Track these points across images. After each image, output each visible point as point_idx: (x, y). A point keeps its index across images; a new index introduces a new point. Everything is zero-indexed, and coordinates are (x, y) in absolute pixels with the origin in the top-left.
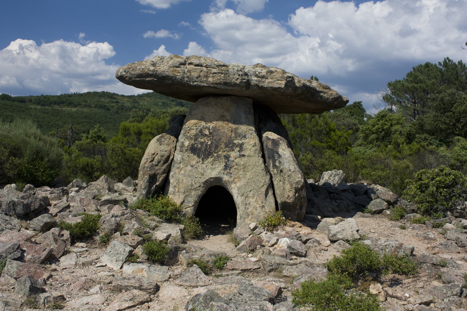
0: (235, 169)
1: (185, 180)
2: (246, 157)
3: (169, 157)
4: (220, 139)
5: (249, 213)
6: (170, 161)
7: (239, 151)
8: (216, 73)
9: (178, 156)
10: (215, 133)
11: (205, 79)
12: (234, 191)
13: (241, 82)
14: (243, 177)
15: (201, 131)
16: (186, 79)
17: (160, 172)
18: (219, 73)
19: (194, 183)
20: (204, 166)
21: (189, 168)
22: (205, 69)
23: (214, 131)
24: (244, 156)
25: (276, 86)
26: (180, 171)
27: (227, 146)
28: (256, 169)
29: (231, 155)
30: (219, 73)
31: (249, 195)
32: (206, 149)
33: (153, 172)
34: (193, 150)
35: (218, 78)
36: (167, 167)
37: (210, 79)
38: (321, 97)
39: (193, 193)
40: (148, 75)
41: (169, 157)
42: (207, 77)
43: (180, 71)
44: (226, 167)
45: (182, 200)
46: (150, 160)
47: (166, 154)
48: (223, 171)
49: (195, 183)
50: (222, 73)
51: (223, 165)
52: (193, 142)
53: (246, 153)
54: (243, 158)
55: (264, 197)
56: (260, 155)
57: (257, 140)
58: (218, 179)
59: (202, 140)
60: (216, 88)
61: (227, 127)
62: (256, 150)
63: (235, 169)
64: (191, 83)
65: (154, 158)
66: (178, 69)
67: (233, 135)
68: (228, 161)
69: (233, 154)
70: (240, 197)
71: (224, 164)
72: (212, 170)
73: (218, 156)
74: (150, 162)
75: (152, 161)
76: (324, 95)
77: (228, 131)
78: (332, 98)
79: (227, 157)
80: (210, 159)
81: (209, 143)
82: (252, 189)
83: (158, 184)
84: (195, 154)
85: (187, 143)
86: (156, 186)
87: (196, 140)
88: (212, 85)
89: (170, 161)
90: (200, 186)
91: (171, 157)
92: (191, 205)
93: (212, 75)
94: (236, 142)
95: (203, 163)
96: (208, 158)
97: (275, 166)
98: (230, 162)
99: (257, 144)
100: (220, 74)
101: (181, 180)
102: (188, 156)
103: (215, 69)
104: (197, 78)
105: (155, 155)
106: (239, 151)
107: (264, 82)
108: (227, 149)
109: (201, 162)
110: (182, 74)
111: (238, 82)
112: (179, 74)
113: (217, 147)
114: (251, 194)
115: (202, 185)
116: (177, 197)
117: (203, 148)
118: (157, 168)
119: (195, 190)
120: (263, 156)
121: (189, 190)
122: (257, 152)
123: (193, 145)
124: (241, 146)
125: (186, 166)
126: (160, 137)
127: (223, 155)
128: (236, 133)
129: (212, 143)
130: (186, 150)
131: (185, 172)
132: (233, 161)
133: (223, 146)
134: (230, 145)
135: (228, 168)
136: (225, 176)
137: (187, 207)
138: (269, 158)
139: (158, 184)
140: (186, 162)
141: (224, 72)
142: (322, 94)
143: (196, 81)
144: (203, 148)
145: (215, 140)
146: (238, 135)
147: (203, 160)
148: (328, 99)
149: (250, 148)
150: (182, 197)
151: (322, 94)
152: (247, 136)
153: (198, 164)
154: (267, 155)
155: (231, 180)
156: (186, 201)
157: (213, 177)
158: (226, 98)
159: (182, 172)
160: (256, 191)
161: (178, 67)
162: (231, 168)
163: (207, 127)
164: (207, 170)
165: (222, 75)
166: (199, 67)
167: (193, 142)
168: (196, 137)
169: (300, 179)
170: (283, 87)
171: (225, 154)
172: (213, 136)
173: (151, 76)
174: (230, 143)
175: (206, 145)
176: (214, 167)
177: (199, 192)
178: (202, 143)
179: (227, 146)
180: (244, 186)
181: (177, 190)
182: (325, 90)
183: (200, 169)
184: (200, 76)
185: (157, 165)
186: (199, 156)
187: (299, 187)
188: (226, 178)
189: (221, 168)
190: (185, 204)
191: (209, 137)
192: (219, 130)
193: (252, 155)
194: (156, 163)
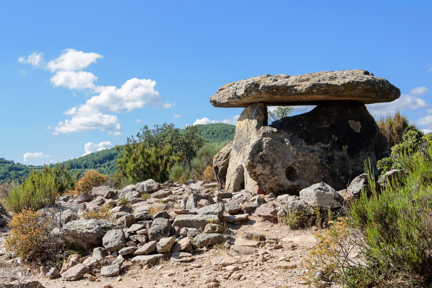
17: (221, 164)
38: (296, 90)
75: (217, 158)
78: (306, 89)
142: (295, 88)
148: (302, 90)
151: (295, 88)
182: (300, 83)
185: (220, 160)
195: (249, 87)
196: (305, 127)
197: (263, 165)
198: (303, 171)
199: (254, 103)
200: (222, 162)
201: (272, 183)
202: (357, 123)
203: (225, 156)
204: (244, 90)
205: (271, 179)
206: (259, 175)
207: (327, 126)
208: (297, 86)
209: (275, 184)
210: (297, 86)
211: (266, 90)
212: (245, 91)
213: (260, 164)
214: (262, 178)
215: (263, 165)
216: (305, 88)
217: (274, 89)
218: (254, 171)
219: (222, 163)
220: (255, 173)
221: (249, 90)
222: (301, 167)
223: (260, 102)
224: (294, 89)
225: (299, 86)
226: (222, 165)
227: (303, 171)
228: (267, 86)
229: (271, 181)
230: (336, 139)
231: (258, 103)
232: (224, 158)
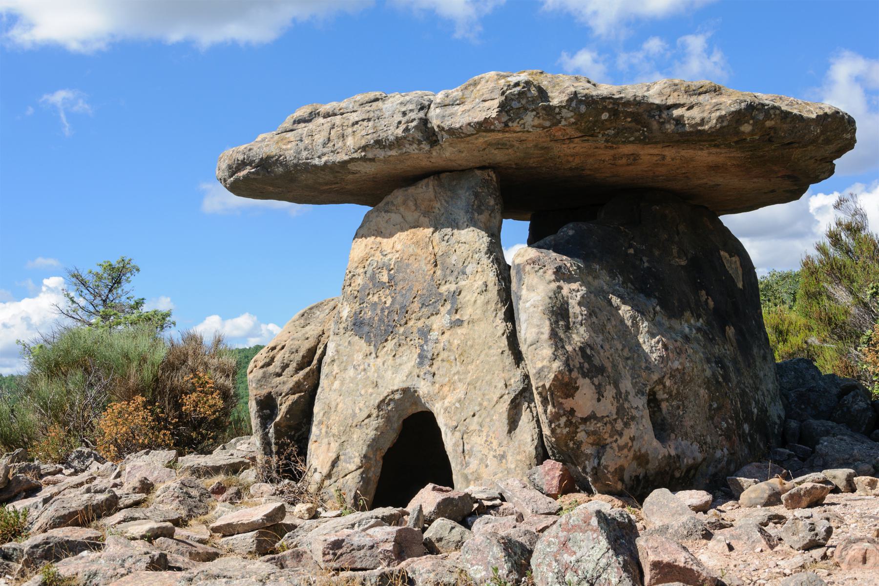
0: (443, 360)
1: (340, 406)
2: (465, 324)
3: (312, 351)
5: (470, 477)
6: (315, 362)
7: (449, 313)
8: (357, 123)
10: (401, 276)
13: (406, 130)
14: (460, 380)
15: (373, 278)
16: (304, 154)
18: (363, 120)
19: (357, 411)
20: (379, 361)
21: (351, 372)
23: (398, 271)
24: (459, 323)
25: (480, 117)
26: (333, 383)
28: (487, 355)
29: (435, 327)
30: (363, 120)
31: (472, 428)
33: (264, 392)
34: (358, 325)
35: (364, 133)
36: (307, 376)
37: (350, 142)
38: (679, 121)
39: (355, 436)
43: (292, 139)
45: (333, 456)
46: (260, 364)
47: (307, 345)
48: (416, 371)
49: (360, 409)
50: (369, 120)
51: (416, 356)
53: (466, 314)
54: (459, 331)
55: (506, 429)
56: (501, 314)
58: (409, 393)
61: (425, 255)
63: (443, 360)
64: (316, 161)
65: (273, 359)
66: (290, 134)
68: (426, 342)
69: (439, 322)
70: (449, 434)
71: (418, 351)
74: (262, 367)
75: (268, 364)
76: (687, 114)
77: (426, 264)
78: (721, 118)
79: (425, 333)
80: (390, 345)
82: (477, 408)
83: (278, 419)
86: (276, 425)
88: (355, 155)
89: (315, 362)
90: (369, 416)
91: (319, 352)
92: (352, 467)
93: (350, 130)
95: (377, 357)
96: (386, 340)
98: (429, 343)
99: (491, 285)
100: (365, 123)
101: (333, 405)
103: (354, 114)
104: (324, 145)
105: (275, 351)
106: (449, 313)
107: (451, 115)
109: (374, 355)
110: (294, 143)
111: (399, 132)
112: (289, 146)
114: (474, 424)
115: (375, 413)
116: (324, 447)
118: (278, 380)
121: (348, 429)
122: (492, 306)
125: (345, 369)
130: (346, 329)
131: (342, 384)
132: (437, 342)
133: (416, 306)
134: (432, 301)
136: (423, 383)
139: (278, 419)
141: (371, 115)
142: (676, 113)
143: (324, 154)
144: (376, 318)
146: (448, 272)
148: (703, 121)
149: (473, 299)
150: (335, 446)
151: (676, 113)
152: (468, 270)
153: (367, 361)
156: (342, 457)
157: (395, 388)
158: (425, 181)
159: (337, 384)
160: (484, 414)
162: (432, 359)
164: (386, 371)
165: (371, 124)
169: (545, 363)
170: (494, 115)
171: (420, 324)
175: (382, 310)
176: (398, 361)
180: (457, 405)
181: (324, 431)
182: (694, 99)
183: (371, 373)
187: (547, 386)
188: (423, 388)
189: (412, 363)
190: (341, 464)
192: (408, 265)
193: (476, 317)
194: (278, 370)
195: (521, 94)
196: (645, 259)
197: (596, 381)
198: (678, 407)
199: (451, 171)
200: (289, 380)
201: (625, 451)
202: (733, 259)
203: (298, 357)
204: (496, 103)
205: (621, 434)
206: (585, 420)
207: (683, 263)
208: (683, 105)
209: (631, 455)
210: (683, 105)
211: (583, 109)
212: (503, 107)
213: (587, 380)
214: (588, 433)
215: (596, 381)
216: (718, 114)
217: (605, 109)
218: (568, 403)
219: (291, 384)
220: (572, 412)
221: (515, 104)
222: (675, 392)
223: (482, 168)
224: (671, 117)
225: (691, 108)
226: (293, 391)
227: (678, 407)
228: (586, 96)
229: (622, 441)
230: (711, 303)
231: (471, 169)
232: (293, 365)
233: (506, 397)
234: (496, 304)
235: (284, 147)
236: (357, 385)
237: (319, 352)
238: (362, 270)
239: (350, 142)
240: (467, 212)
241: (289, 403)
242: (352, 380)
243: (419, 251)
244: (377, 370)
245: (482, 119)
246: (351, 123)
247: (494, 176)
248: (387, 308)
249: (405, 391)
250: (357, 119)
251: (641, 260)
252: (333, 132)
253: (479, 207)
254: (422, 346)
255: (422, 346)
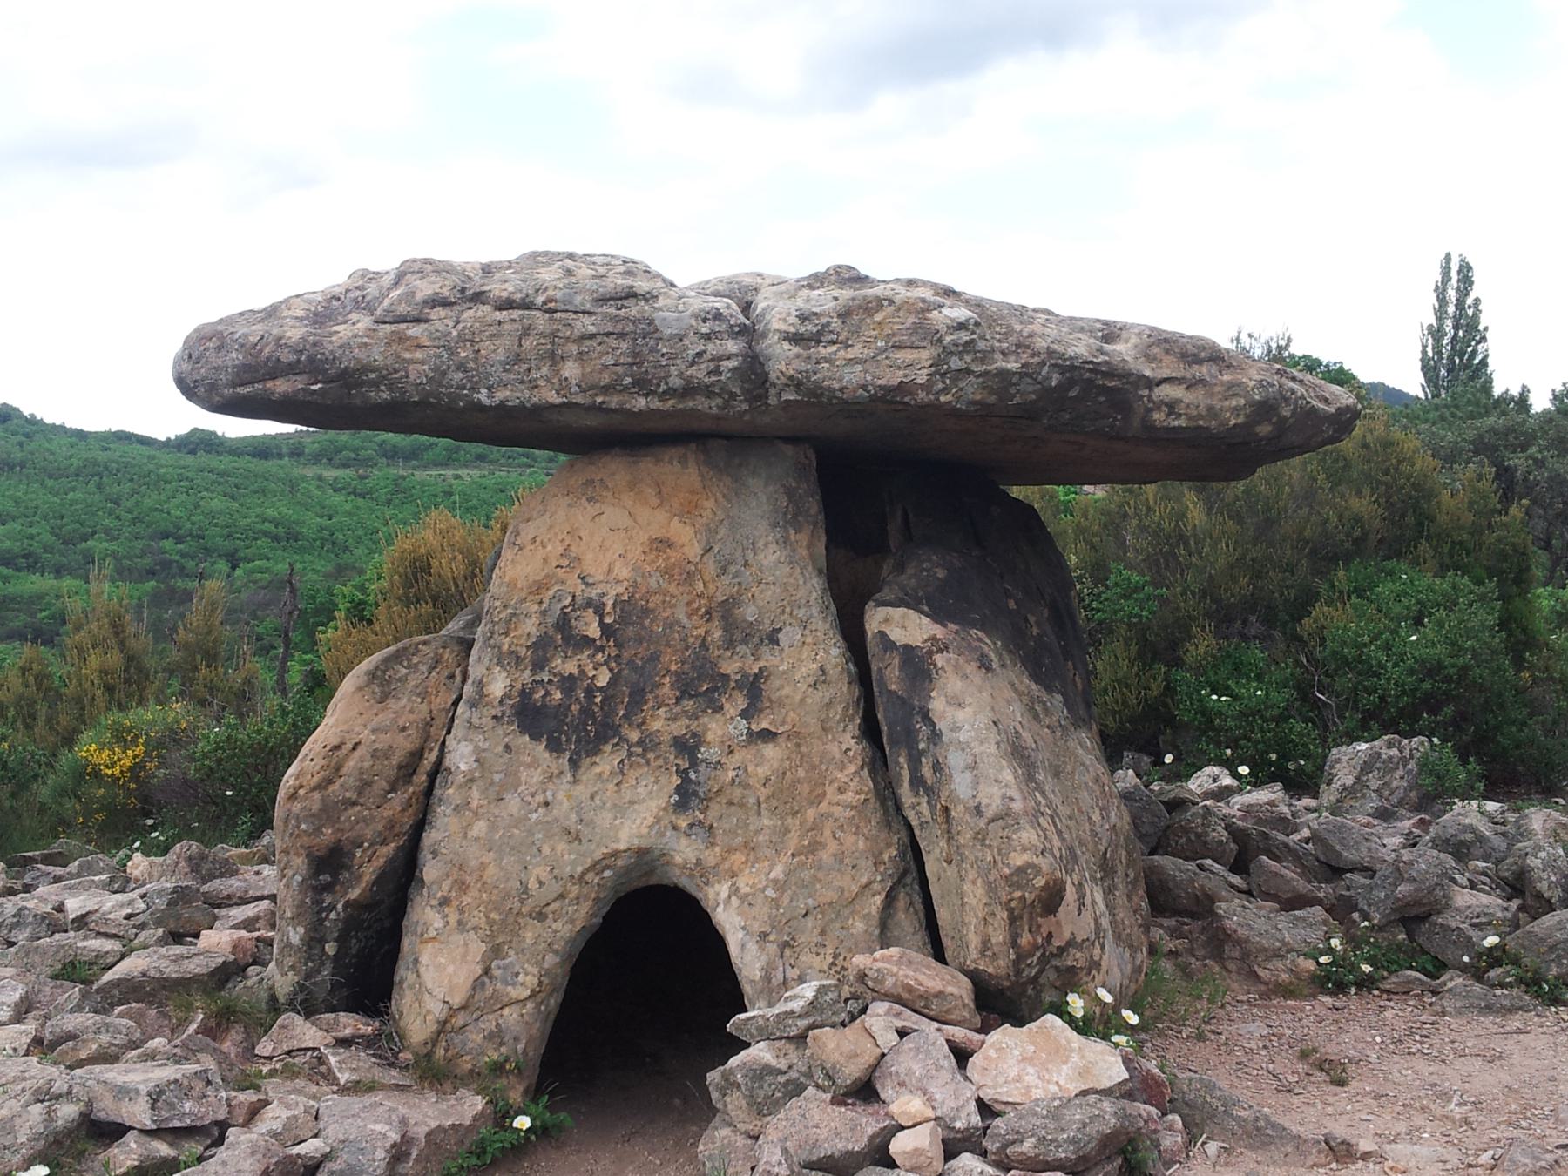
0: (730, 803)
1: (491, 870)
2: (781, 740)
3: (418, 754)
4: (654, 658)
6: (421, 778)
7: (745, 714)
8: (592, 336)
9: (461, 756)
11: (545, 370)
12: (730, 921)
15: (563, 624)
18: (608, 334)
20: (581, 791)
22: (540, 320)
23: (624, 619)
24: (767, 736)
27: (685, 689)
29: (710, 737)
32: (586, 712)
34: (530, 716)
40: (277, 370)
41: (418, 754)
42: (554, 358)
44: (686, 796)
47: (404, 744)
49: (541, 883)
50: (622, 335)
52: (526, 676)
57: (834, 654)
59: (571, 668)
60: (600, 409)
61: (686, 598)
62: (829, 705)
64: (483, 396)
65: (338, 768)
66: (415, 330)
67: (718, 634)
68: (694, 763)
69: (722, 727)
70: (752, 947)
72: (625, 812)
73: (648, 744)
79: (688, 747)
80: (607, 761)
81: (603, 679)
83: (354, 894)
84: (535, 737)
85: (498, 686)
86: (347, 905)
87: (539, 665)
88: (580, 399)
90: (562, 896)
93: (574, 348)
94: (730, 667)
95: (576, 781)
97: (917, 782)
98: (702, 768)
99: (833, 673)
100: (613, 342)
102: (507, 748)
103: (586, 320)
106: (745, 714)
108: (688, 704)
112: (418, 355)
113: (638, 698)
117: (575, 708)
119: (541, 916)
120: (870, 731)
121: (511, 919)
123: (525, 694)
124: (754, 687)
126: (387, 661)
127: (666, 738)
128: (729, 623)
129: (614, 681)
131: (493, 827)
133: (667, 690)
134: (702, 686)
135: (694, 803)
136: (684, 841)
137: (505, 1000)
138: (894, 743)
140: (497, 778)
144: (575, 708)
145: (630, 662)
147: (574, 764)
154: (887, 725)
155: (711, 857)
159: (480, 828)
161: (417, 321)
163: (589, 603)
166: (516, 314)
167: (526, 676)
168: (541, 651)
171: (679, 728)
172: (618, 645)
173: (291, 369)
174: (701, 678)
175: (590, 692)
177: (557, 925)
178: (568, 683)
179: (685, 689)
181: (453, 918)
184: (518, 359)
186: (554, 747)
188: (684, 851)
191: (602, 649)
192: (646, 612)
233: (876, 886)
234: (846, 709)
235: (407, 355)
236: (530, 833)
237: (432, 757)
238: (536, 607)
239: (571, 370)
240: (775, 525)
241: (379, 862)
242: (517, 822)
243: (672, 588)
244: (579, 808)
245: (895, 381)
246: (577, 333)
247: (813, 457)
248: (601, 689)
249: (641, 852)
250: (592, 329)
251: (1027, 620)
252: (526, 344)
253: (795, 516)
254: (686, 772)
255: (686, 772)
